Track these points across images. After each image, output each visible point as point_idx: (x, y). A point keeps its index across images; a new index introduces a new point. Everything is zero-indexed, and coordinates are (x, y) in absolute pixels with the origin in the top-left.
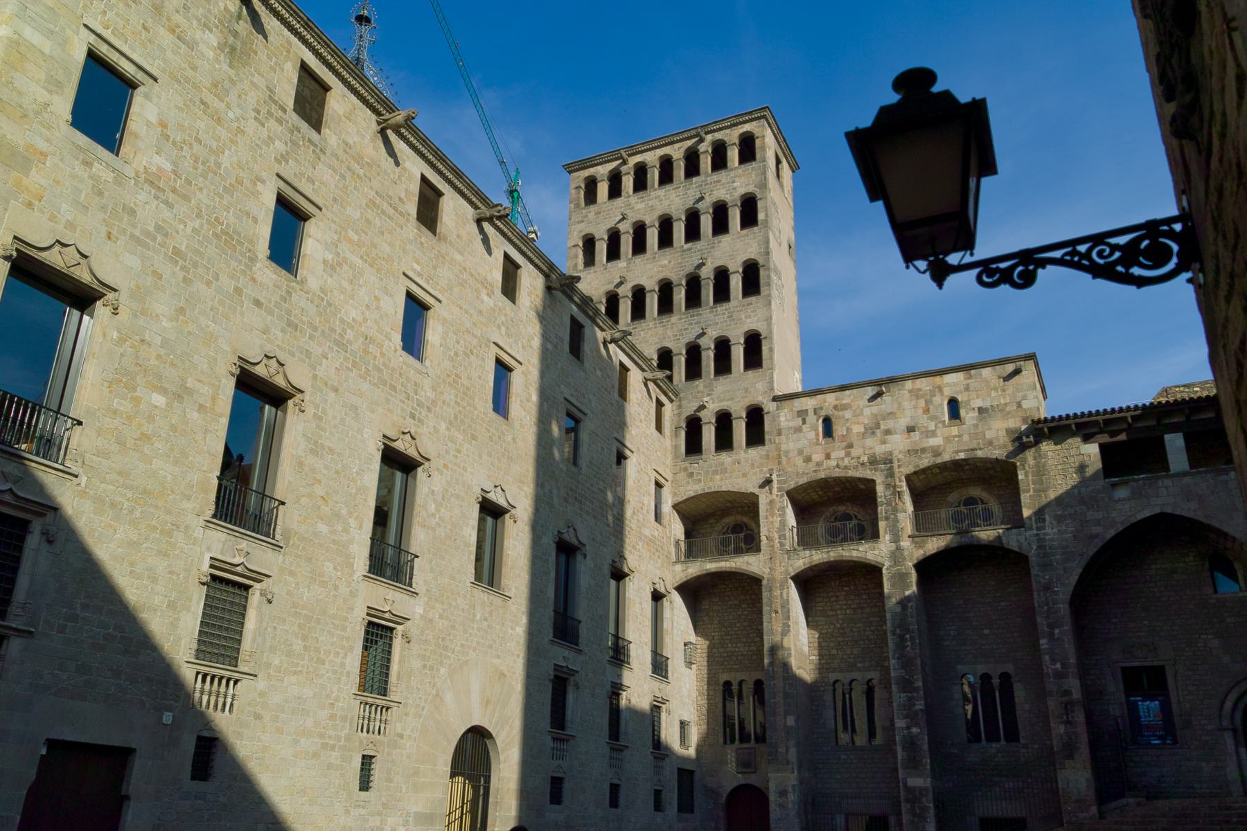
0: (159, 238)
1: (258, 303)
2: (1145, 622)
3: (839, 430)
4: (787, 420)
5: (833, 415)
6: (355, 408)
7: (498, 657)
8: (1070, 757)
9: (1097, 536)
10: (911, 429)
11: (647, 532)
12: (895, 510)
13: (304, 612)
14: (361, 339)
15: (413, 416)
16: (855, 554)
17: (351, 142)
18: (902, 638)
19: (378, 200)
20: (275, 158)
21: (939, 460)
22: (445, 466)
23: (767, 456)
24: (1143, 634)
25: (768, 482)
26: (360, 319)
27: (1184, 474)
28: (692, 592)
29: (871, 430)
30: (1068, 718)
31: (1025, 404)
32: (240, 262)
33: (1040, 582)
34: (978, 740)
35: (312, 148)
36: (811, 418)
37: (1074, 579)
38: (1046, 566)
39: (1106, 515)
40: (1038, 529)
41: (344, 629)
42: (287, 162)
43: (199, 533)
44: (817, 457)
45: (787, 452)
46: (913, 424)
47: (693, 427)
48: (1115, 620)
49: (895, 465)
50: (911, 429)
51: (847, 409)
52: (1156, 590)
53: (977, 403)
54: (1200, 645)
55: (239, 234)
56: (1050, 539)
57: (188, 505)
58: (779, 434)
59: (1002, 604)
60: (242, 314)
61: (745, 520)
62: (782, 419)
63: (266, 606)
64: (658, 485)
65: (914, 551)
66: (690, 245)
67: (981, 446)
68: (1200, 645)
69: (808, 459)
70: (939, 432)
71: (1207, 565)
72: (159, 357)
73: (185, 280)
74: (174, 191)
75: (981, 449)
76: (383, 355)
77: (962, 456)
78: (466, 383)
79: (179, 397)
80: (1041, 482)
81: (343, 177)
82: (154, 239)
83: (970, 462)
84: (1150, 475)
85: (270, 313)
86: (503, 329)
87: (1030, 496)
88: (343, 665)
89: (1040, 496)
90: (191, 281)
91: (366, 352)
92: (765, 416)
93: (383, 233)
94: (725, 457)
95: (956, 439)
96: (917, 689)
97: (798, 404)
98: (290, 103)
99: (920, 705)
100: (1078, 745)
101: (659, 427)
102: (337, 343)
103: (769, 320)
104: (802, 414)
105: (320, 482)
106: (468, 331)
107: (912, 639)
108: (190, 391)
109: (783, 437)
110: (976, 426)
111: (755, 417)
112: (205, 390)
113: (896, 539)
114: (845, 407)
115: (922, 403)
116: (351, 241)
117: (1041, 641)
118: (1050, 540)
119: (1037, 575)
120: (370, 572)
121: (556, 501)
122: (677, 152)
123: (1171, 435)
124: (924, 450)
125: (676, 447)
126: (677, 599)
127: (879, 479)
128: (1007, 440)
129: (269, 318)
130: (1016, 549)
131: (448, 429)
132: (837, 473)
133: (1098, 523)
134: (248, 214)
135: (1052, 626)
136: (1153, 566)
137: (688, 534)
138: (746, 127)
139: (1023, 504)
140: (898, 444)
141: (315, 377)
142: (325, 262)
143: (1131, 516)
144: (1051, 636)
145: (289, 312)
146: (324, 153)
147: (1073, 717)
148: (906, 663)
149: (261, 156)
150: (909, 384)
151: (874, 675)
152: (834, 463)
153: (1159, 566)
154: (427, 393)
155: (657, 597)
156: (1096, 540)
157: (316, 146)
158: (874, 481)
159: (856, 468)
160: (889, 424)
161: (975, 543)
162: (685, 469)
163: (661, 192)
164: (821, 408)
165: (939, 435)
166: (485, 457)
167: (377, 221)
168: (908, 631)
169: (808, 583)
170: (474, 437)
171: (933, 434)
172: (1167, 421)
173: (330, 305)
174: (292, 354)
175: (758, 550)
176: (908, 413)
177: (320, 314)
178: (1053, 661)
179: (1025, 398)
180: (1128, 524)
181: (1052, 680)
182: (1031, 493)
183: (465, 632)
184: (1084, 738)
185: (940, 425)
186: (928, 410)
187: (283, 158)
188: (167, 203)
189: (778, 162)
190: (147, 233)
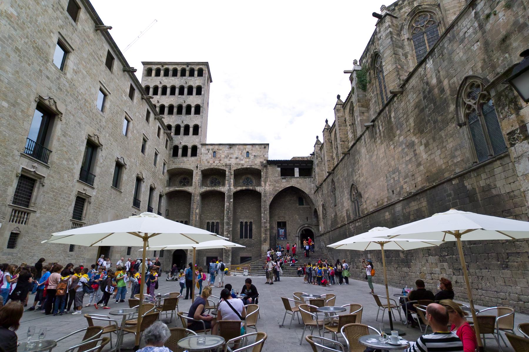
0: (10, 41)
1: (48, 78)
3: (218, 156)
6: (79, 123)
7: (117, 210)
8: (265, 242)
9: (277, 190)
10: (237, 158)
11: (160, 177)
12: (230, 179)
13: (56, 191)
14: (84, 100)
15: (98, 130)
16: (218, 189)
17: (86, 30)
18: (228, 212)
19: (93, 54)
20: (59, 26)
21: (243, 167)
22: (107, 148)
23: (197, 160)
25: (197, 167)
26: (84, 93)
27: (298, 178)
28: (171, 196)
29: (227, 157)
31: (265, 156)
32: (42, 60)
34: (243, 238)
35: (72, 27)
36: (211, 151)
37: (271, 200)
38: (265, 196)
41: (69, 198)
42: (63, 29)
43: (18, 158)
44: (211, 162)
45: (203, 160)
47: (176, 148)
49: (232, 167)
50: (237, 158)
53: (254, 154)
55: (43, 50)
57: (15, 147)
58: (201, 154)
60: (42, 80)
61: (187, 177)
63: (41, 187)
64: (164, 164)
65: (233, 189)
66: (180, 96)
69: (208, 162)
72: (6, 88)
73: (19, 60)
74: (17, 24)
76: (90, 107)
78: (116, 122)
79: (14, 106)
81: (82, 41)
82: (8, 41)
85: (52, 82)
86: (128, 108)
88: (67, 210)
90: (22, 62)
91: (85, 105)
93: (94, 65)
94: (185, 159)
96: (231, 225)
97: (207, 147)
98: (66, 8)
99: (231, 229)
101: (166, 147)
102: (75, 99)
103: (202, 122)
104: (208, 150)
105: (65, 146)
106: (118, 106)
107: (231, 212)
108: (19, 104)
109: (202, 155)
110: (253, 160)
111: (195, 149)
112: (25, 105)
113: (230, 186)
114: (220, 150)
115: (240, 152)
116: (83, 65)
120: (80, 179)
121: (138, 164)
122: (179, 68)
124: (239, 164)
125: (170, 154)
126: (164, 197)
127: (227, 170)
129: (52, 84)
131: (109, 136)
132: (216, 167)
134: (47, 43)
135: (265, 211)
137: (170, 179)
138: (201, 66)
140: (233, 161)
141: (66, 109)
142: (73, 69)
144: (264, 213)
145: (59, 84)
146: (76, 31)
148: (229, 218)
149: (53, 23)
150: (237, 146)
151: (218, 221)
152: (215, 164)
154: (103, 123)
155: (161, 196)
157: (74, 27)
158: (225, 170)
159: (221, 166)
160: (231, 156)
162: (172, 160)
163: (173, 78)
166: (119, 147)
167: (93, 61)
168: (230, 210)
169: (205, 196)
170: (116, 141)
171: (242, 160)
172: (296, 165)
173: (74, 85)
174: (59, 99)
175: (191, 185)
176: (236, 154)
177: (70, 88)
178: (264, 219)
179: (265, 154)
183: (108, 202)
184: (269, 238)
187: (61, 27)
188: (14, 28)
189: (208, 79)
190: (5, 38)
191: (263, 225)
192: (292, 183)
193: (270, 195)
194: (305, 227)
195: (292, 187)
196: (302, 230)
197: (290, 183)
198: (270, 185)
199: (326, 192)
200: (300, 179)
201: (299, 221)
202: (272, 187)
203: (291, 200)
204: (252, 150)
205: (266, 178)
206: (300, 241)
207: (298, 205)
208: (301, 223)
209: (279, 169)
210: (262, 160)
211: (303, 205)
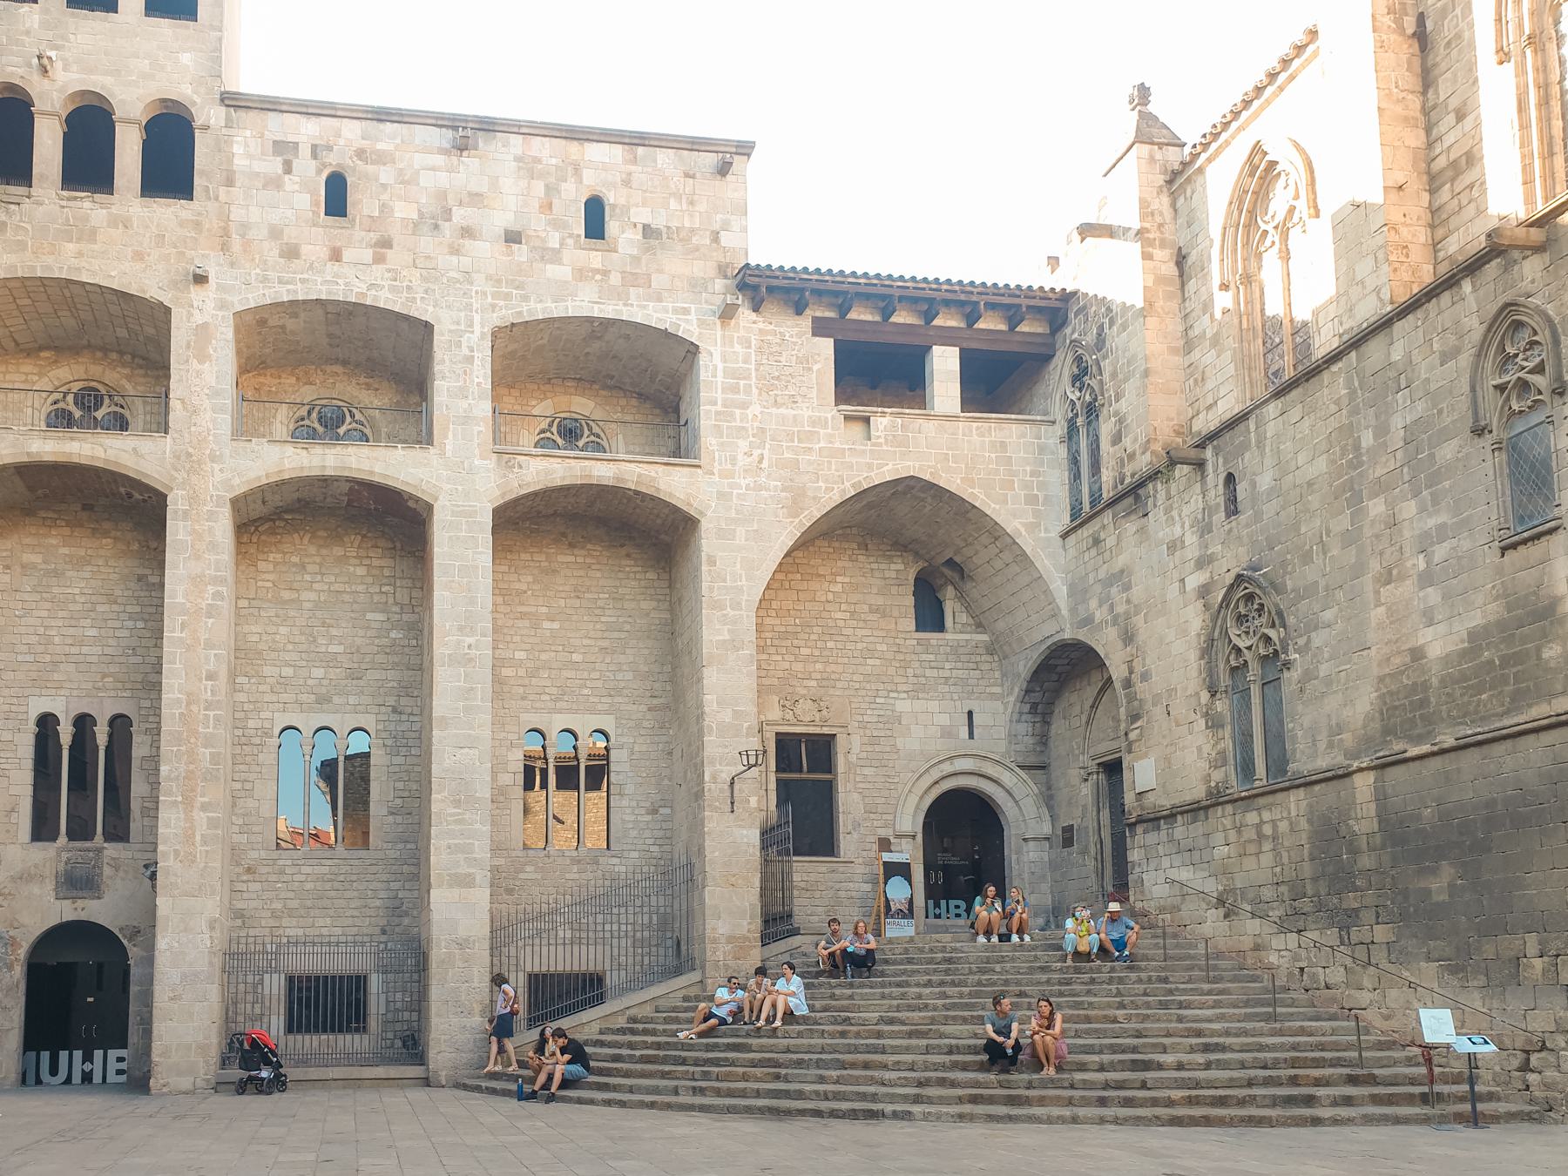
4: (250, 156)
5: (354, 169)
10: (513, 238)
29: (435, 219)
36: (305, 165)
46: (517, 228)
50: (513, 238)
51: (385, 164)
62: (237, 149)
70: (567, 255)
92: (197, 133)
95: (598, 277)
104: (285, 149)
110: (636, 260)
114: (382, 159)
164: (330, 148)
165: (565, 261)
171: (554, 256)
185: (570, 241)
186: (550, 206)
204: (627, 182)
209: (826, 346)
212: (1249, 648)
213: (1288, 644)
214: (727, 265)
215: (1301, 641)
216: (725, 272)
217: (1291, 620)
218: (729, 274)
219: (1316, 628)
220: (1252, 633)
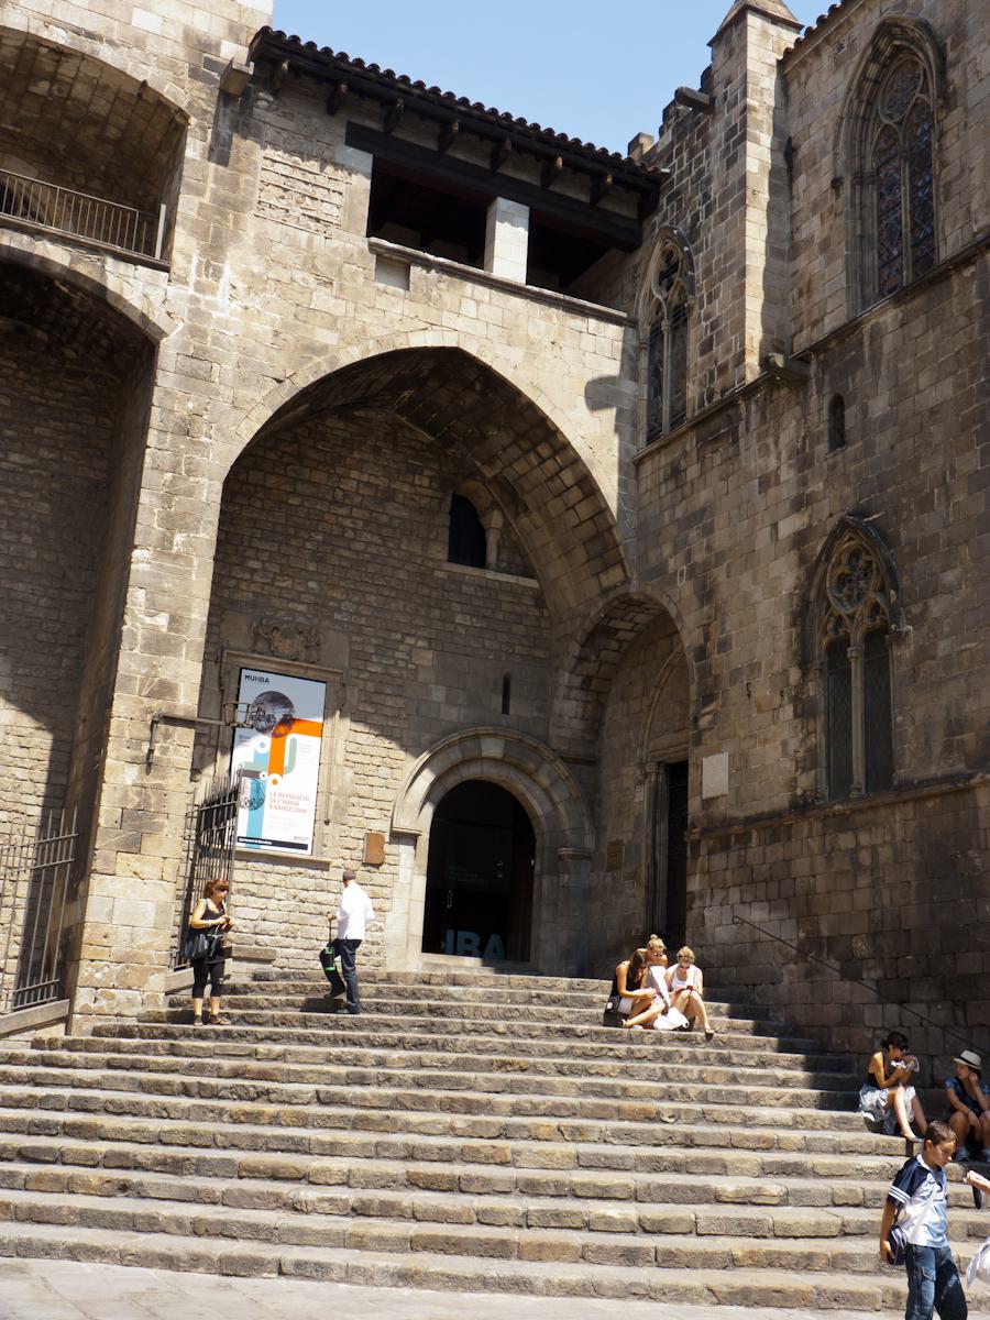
2: (312, 584)
9: (323, 349)
24: (302, 608)
30: (151, 751)
33: (172, 411)
38: (197, 375)
39: (351, 313)
40: (199, 287)
48: (253, 564)
52: (348, 523)
54: (398, 655)
56: (218, 322)
59: (15, 457)
67: (115, 37)
68: (398, 655)
71: (447, 506)
75: (111, 43)
77: (59, 37)
80: (234, 185)
83: (68, 70)
84: (456, 265)
87: (201, 206)
89: (224, 216)
100: (160, 819)
117: (136, 554)
118: (225, 324)
119: (167, 393)
123: (510, 203)
128: (181, 53)
130: (136, 319)
133: (332, 323)
136: (354, 474)
139: (178, 218)
143: (398, 333)
144: (164, 547)
147: (165, 751)
153: (365, 478)
156: (317, 359)
161: (34, 264)
172: (507, 170)
178: (153, 608)
180: (391, 349)
181: (137, 651)
182: (206, 199)
191: (130, 662)
192: (460, 323)
193: (244, 381)
194: (479, 759)
195: (453, 366)
196: (452, 782)
197: (448, 319)
198: (255, 283)
199: (947, 389)
200: (537, 309)
201: (438, 694)
202: (268, 315)
203: (389, 496)
205: (228, 206)
206: (420, 883)
207: (440, 551)
208: (452, 714)
210: (207, 24)
211: (480, 561)
212: (852, 617)
213: (900, 614)
214: (241, 28)
215: (916, 609)
216: (238, 35)
217: (904, 582)
218: (243, 39)
219: (934, 593)
220: (855, 598)
